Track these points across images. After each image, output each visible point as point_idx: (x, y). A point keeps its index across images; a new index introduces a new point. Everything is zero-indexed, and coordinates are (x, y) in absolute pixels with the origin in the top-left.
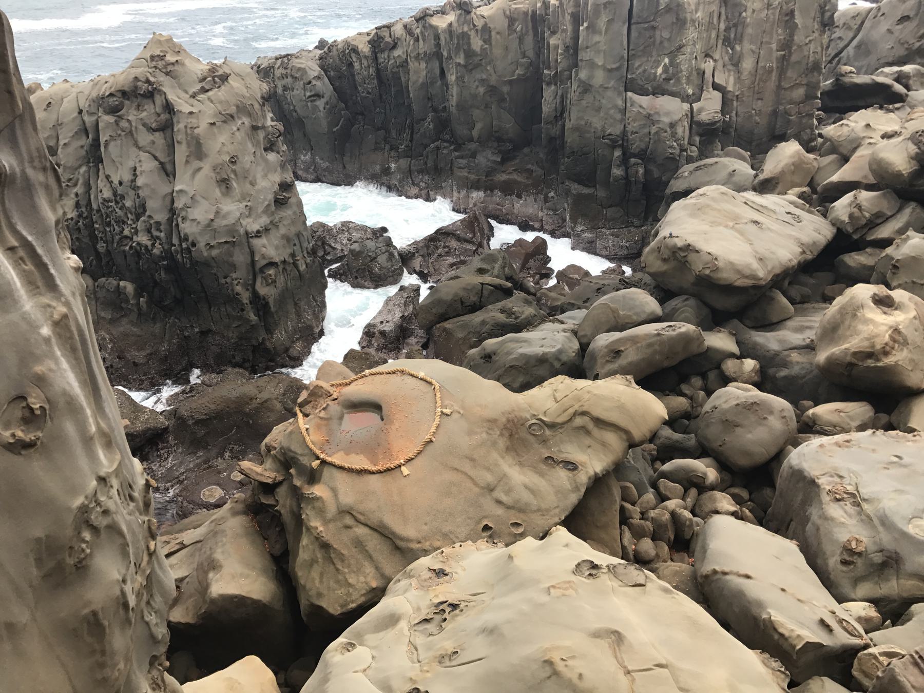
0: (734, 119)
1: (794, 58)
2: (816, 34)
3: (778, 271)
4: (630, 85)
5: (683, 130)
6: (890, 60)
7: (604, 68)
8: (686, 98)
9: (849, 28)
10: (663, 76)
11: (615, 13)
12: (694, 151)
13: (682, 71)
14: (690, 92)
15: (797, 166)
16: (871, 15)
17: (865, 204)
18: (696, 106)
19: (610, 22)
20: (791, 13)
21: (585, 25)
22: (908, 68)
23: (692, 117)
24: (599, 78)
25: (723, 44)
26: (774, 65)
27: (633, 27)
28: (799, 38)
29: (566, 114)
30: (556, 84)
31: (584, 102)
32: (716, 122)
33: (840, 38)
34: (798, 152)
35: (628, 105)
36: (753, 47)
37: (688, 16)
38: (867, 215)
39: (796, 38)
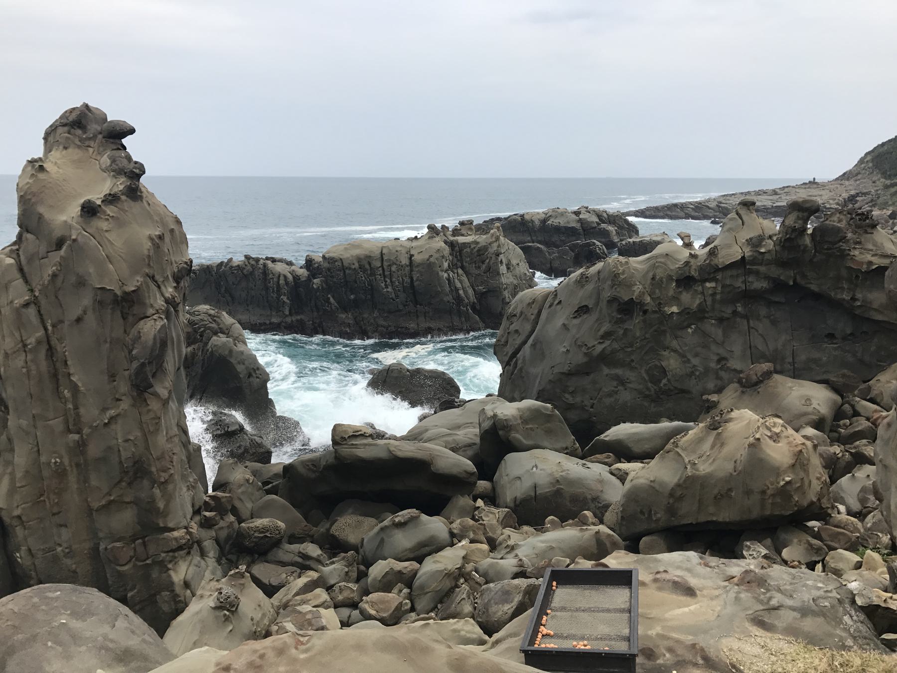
1: (94, 450)
2: (125, 405)
9: (527, 319)
16: (547, 305)
26: (66, 461)
33: (517, 331)
36: (24, 423)
39: (82, 411)
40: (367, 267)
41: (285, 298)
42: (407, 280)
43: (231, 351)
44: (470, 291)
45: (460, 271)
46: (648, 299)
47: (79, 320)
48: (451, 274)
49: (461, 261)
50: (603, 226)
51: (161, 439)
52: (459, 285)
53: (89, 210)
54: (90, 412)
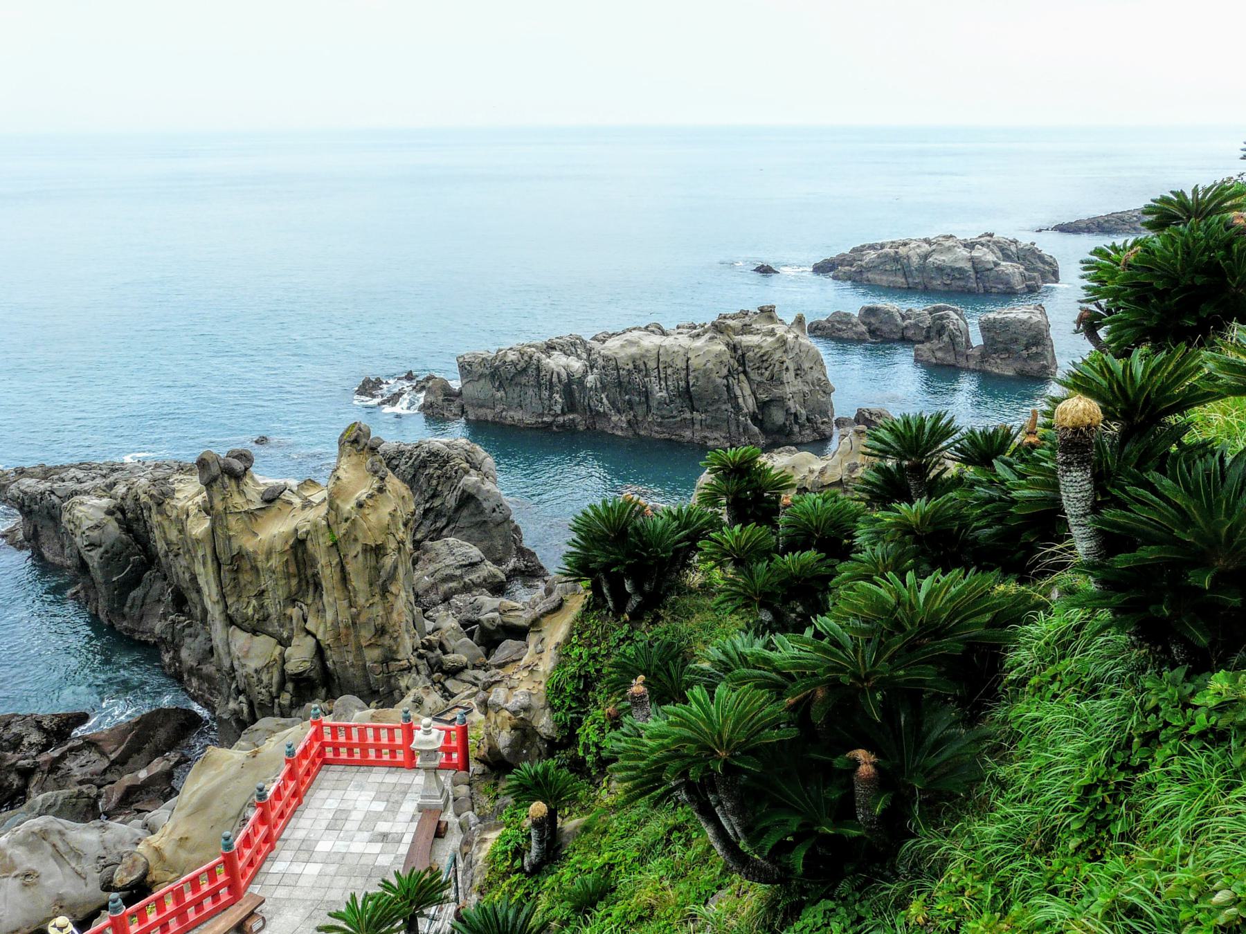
1: (363, 618)
2: (377, 598)
10: (256, 617)
40: (642, 367)
41: (557, 396)
42: (682, 384)
43: (479, 489)
44: (751, 401)
45: (742, 377)
48: (731, 379)
49: (743, 364)
51: (395, 615)
52: (738, 393)
53: (360, 505)
54: (361, 600)
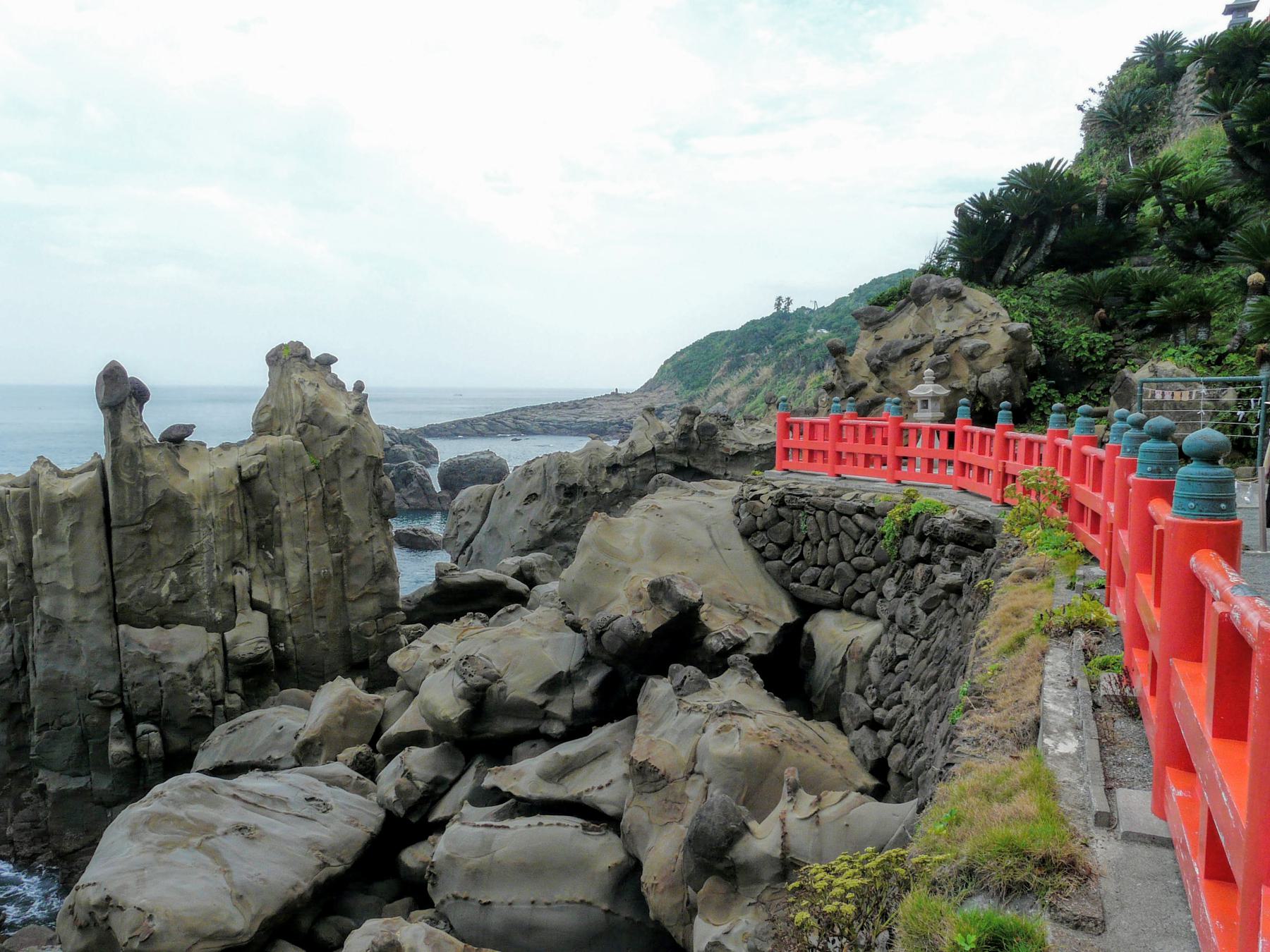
0: (291, 647)
2: (377, 530)
3: (270, 911)
4: (118, 616)
5: (213, 673)
6: (525, 546)
7: (75, 592)
8: (212, 626)
10: (173, 597)
11: (82, 514)
12: (234, 701)
13: (200, 589)
14: (218, 616)
15: (350, 715)
17: (417, 770)
18: (229, 636)
19: (77, 527)
20: (338, 504)
21: (39, 532)
22: (530, 558)
23: (225, 652)
24: (70, 608)
25: (259, 547)
27: (114, 532)
28: (356, 535)
29: (30, 665)
30: (10, 621)
31: (55, 646)
32: (260, 657)
33: (467, 523)
34: (347, 694)
35: (122, 644)
36: (299, 550)
37: (195, 513)
38: (421, 785)
39: (350, 535)
46: (587, 484)
47: (353, 477)
50: (398, 446)
